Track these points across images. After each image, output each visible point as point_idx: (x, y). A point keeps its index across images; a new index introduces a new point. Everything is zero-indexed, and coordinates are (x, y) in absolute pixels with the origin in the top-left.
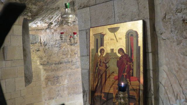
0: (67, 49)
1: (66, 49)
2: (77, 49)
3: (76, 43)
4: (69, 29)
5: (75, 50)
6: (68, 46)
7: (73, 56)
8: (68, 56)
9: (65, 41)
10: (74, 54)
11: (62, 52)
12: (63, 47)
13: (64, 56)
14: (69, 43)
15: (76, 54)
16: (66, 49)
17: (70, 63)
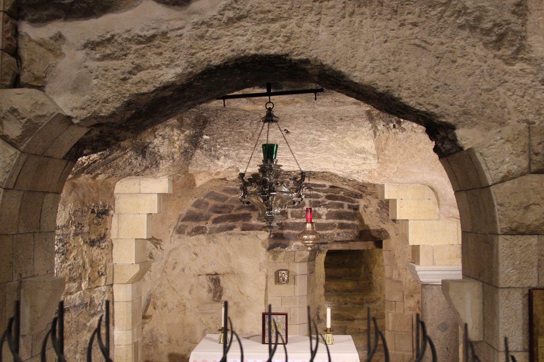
0: (82, 258)
1: (80, 257)
2: (105, 258)
3: (102, 236)
4: (91, 190)
5: (100, 260)
6: (85, 248)
7: (94, 282)
8: (83, 285)
9: (79, 231)
10: (96, 274)
11: (68, 271)
12: (71, 253)
13: (75, 285)
14: (88, 240)
15: (102, 274)
16: (80, 257)
17: (88, 308)
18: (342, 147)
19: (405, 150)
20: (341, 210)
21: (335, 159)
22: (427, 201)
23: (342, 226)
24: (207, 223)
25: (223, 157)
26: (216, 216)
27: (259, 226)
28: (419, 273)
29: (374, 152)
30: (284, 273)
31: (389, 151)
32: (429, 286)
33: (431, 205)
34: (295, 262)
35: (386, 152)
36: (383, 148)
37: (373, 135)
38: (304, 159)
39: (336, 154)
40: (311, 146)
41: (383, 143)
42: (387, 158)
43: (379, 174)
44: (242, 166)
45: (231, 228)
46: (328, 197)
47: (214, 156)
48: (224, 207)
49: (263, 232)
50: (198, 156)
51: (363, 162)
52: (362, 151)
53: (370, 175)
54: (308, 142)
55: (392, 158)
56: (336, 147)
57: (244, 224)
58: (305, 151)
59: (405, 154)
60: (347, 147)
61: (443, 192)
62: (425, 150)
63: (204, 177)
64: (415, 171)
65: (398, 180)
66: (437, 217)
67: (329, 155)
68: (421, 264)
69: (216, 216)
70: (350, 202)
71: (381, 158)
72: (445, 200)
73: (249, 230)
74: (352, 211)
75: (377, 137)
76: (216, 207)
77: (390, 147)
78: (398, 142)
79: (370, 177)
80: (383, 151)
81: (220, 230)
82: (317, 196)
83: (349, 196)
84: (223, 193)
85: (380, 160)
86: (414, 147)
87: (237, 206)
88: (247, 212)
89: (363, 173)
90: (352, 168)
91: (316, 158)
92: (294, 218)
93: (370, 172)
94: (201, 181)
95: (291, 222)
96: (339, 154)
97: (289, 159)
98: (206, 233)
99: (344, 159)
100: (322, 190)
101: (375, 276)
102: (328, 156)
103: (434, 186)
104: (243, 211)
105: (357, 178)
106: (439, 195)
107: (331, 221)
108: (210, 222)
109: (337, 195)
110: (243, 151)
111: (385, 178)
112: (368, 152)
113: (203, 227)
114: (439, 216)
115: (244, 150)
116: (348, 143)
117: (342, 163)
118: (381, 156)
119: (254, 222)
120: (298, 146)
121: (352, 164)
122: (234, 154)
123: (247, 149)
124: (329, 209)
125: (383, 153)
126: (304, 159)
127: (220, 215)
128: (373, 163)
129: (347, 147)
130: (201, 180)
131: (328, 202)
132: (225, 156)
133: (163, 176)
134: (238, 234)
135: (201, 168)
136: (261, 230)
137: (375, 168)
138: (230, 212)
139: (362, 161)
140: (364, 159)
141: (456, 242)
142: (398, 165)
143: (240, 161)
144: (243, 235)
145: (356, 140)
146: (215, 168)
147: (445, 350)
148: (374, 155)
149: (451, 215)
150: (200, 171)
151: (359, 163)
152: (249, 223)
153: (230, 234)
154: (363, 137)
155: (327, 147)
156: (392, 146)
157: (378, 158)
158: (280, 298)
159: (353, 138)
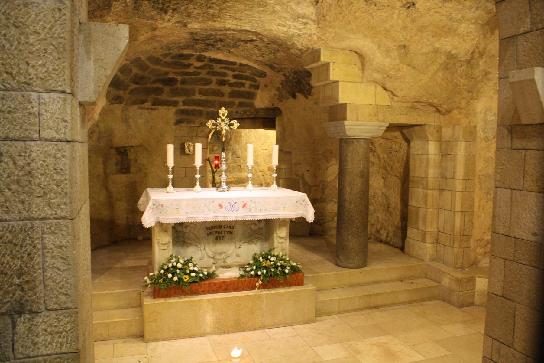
18: (287, 11)
19: (344, 17)
20: (242, 89)
21: (279, 21)
22: (354, 66)
23: (241, 104)
24: (125, 93)
25: (171, 11)
26: (133, 86)
27: (168, 101)
28: (346, 127)
29: (314, 17)
30: (189, 145)
31: (330, 17)
32: (350, 140)
33: (356, 69)
34: (197, 137)
35: (327, 17)
36: (325, 13)
37: (315, 3)
38: (251, 19)
39: (281, 16)
40: (258, 7)
41: (326, 9)
42: (327, 24)
43: (319, 38)
44: (190, 21)
45: (143, 102)
46: (235, 77)
47: (161, 10)
48: (142, 78)
49: (171, 107)
50: (145, 8)
51: (304, 26)
52: (303, 16)
53: (310, 38)
54: (256, 4)
55: (332, 23)
56: (281, 10)
57: (155, 99)
58: (252, 11)
59: (344, 20)
60: (291, 11)
61: (371, 57)
62: (360, 18)
63: (147, 33)
64: (351, 36)
65: (334, 45)
66: (360, 80)
67: (274, 17)
68: (347, 120)
69: (133, 86)
70: (252, 81)
71: (321, 24)
72: (371, 64)
73: (159, 105)
74: (252, 90)
75: (319, 4)
76: (136, 76)
77: (332, 13)
78: (339, 9)
79: (309, 40)
80: (324, 17)
81: (134, 103)
82: (225, 75)
83: (255, 75)
84: (147, 62)
85: (320, 25)
86: (352, 14)
87: (153, 78)
88: (161, 86)
89: (303, 36)
90: (295, 31)
91: (262, 19)
92: (200, 96)
93: (310, 35)
94: (142, 37)
95: (197, 99)
96: (284, 17)
97: (237, 17)
98: (123, 103)
99: (288, 22)
100: (231, 68)
101: (243, 160)
102: (273, 18)
103: (364, 51)
104: (157, 85)
105: (298, 41)
106: (367, 59)
107: (232, 99)
108: (127, 92)
109: (242, 73)
110: (192, 6)
111: (323, 41)
112: (308, 17)
113: (121, 97)
114: (362, 80)
115: (193, 5)
116: (292, 8)
117: (285, 26)
118: (321, 22)
119: (164, 97)
120: (247, 6)
121: (294, 28)
122: (183, 8)
123: (197, 5)
124: (233, 88)
125: (325, 18)
126: (251, 19)
127: (137, 86)
128: (313, 28)
129: (291, 11)
130: (143, 35)
131: (233, 81)
132: (174, 10)
133: (113, 20)
134: (148, 109)
135: (148, 20)
136: (170, 105)
137: (314, 32)
138: (146, 84)
139: (302, 26)
140: (305, 24)
141: (374, 102)
142: (336, 30)
143: (189, 16)
144: (152, 109)
145: (299, 6)
146: (161, 22)
147: (362, 193)
148: (314, 21)
149: (372, 79)
150: (146, 23)
151: (300, 27)
152: (160, 97)
153: (141, 108)
154: (305, 4)
155: (273, 10)
156: (334, 12)
157: (318, 24)
158: (184, 169)
159: (296, 3)
